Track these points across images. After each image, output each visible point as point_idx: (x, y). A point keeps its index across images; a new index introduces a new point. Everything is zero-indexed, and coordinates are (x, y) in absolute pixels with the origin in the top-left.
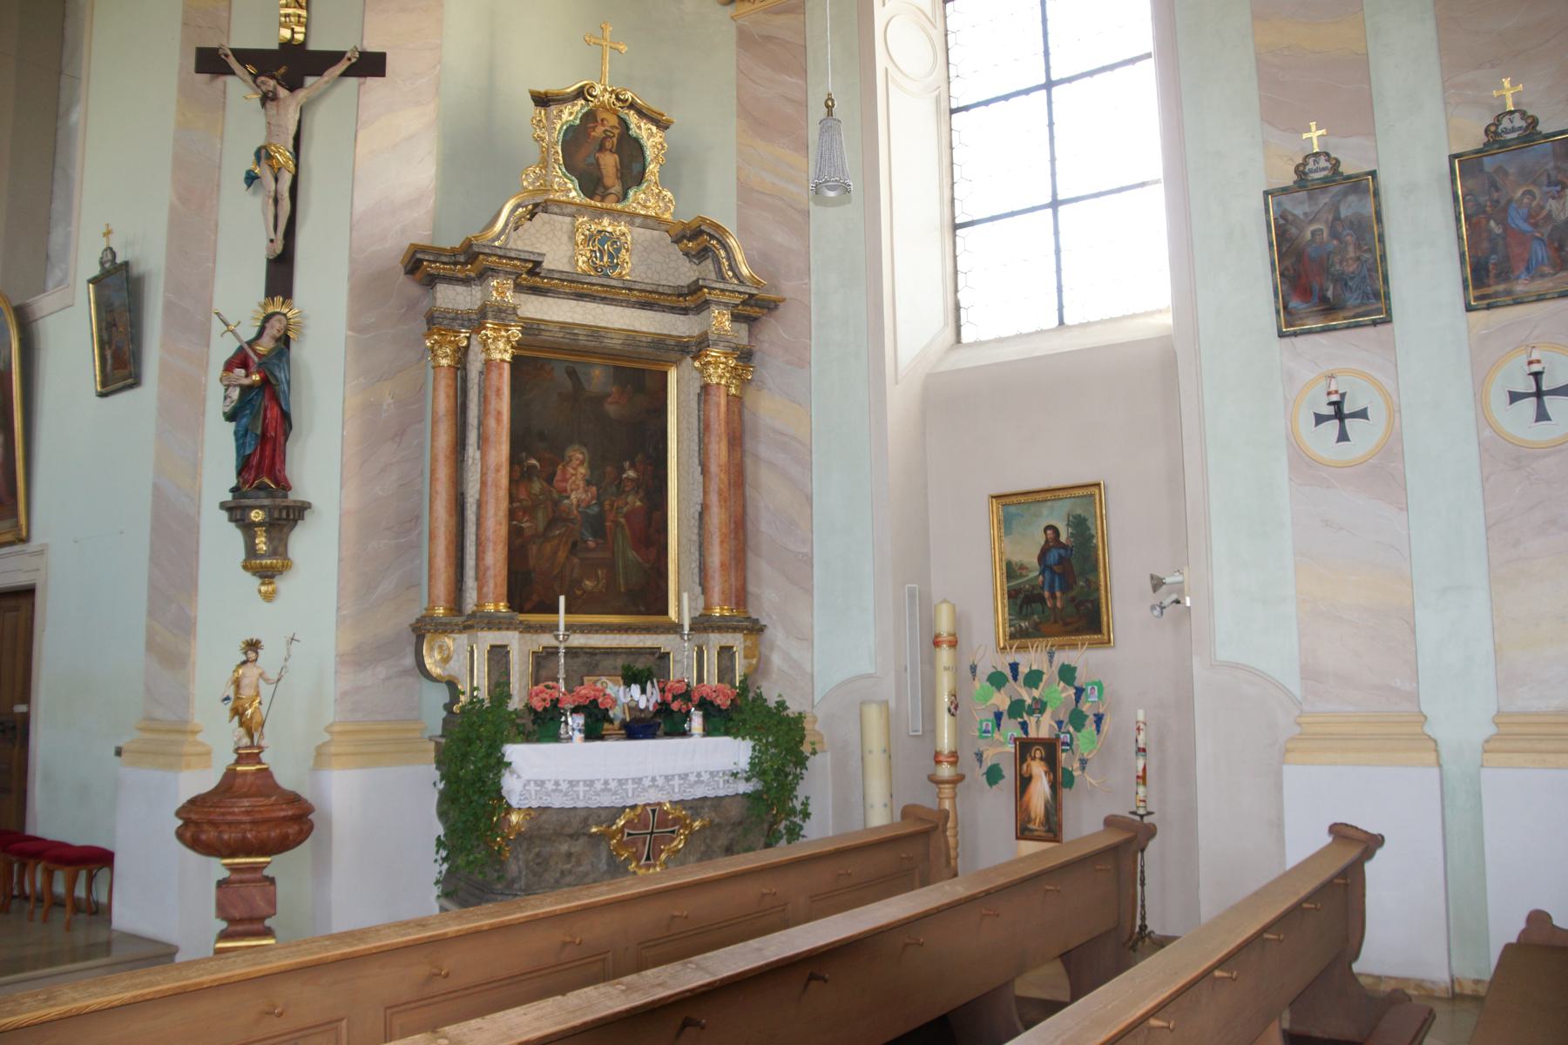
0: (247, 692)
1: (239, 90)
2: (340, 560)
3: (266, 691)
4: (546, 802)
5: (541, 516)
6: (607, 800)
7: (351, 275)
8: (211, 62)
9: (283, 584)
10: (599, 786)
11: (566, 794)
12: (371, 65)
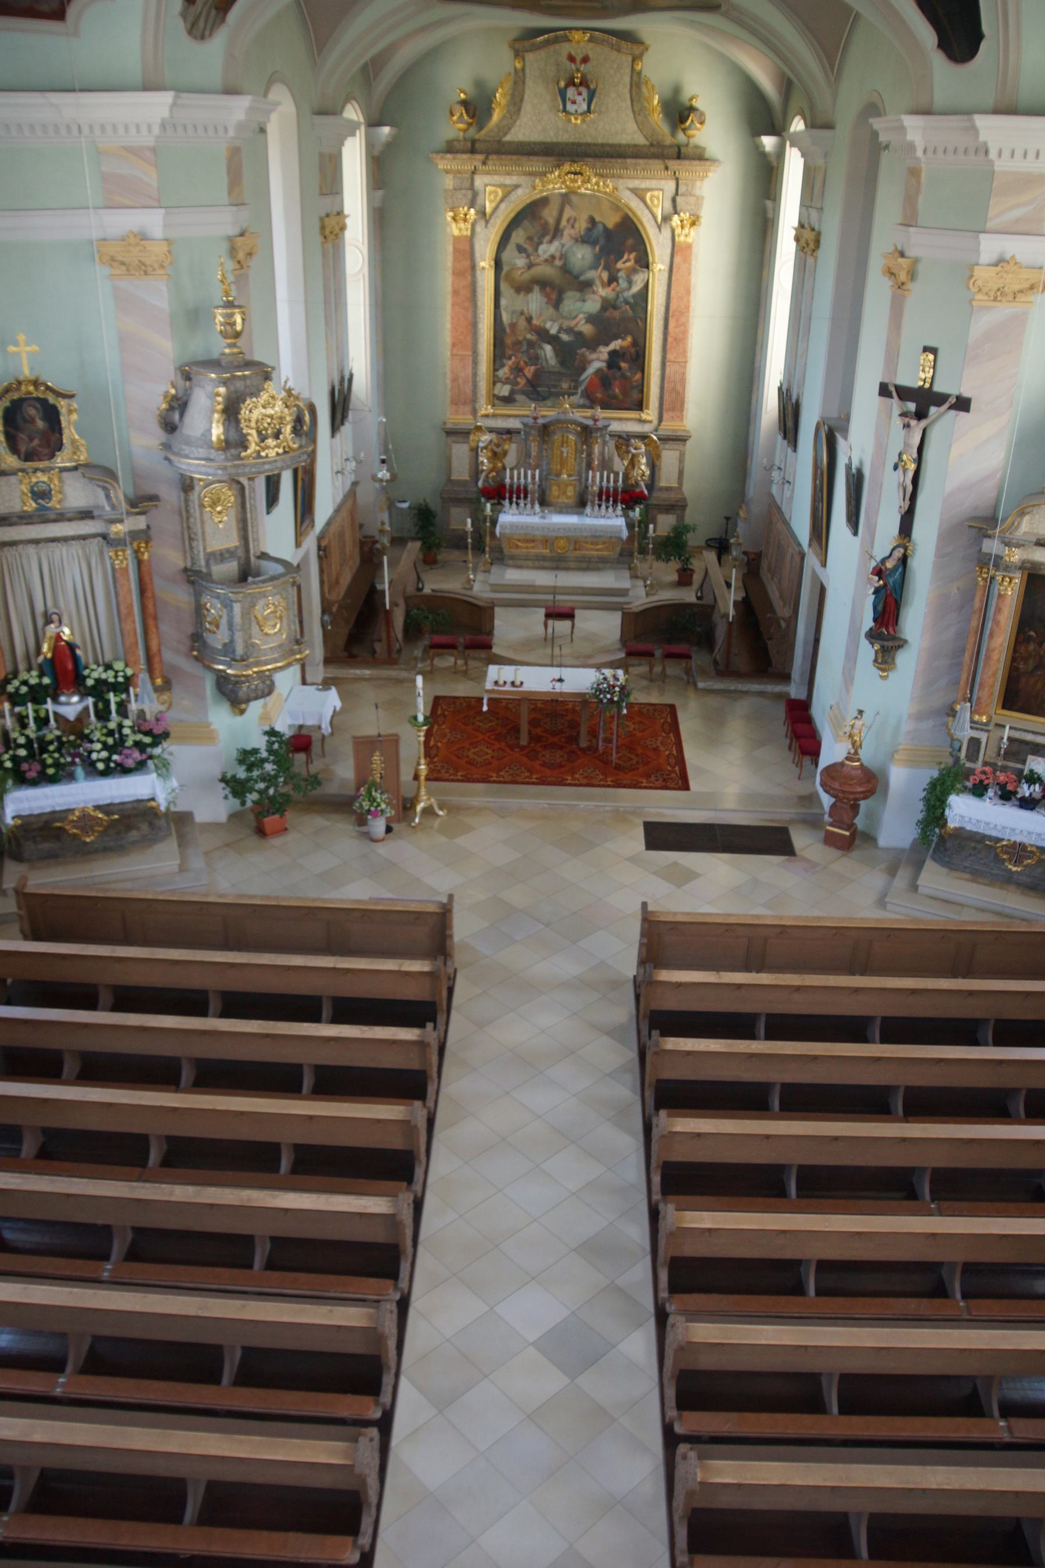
0: (856, 731)
1: (895, 405)
2: (916, 671)
3: (864, 730)
4: (964, 825)
5: (1031, 664)
6: (994, 833)
7: (940, 526)
8: (884, 390)
9: (892, 675)
10: (992, 826)
11: (974, 825)
12: (963, 404)
